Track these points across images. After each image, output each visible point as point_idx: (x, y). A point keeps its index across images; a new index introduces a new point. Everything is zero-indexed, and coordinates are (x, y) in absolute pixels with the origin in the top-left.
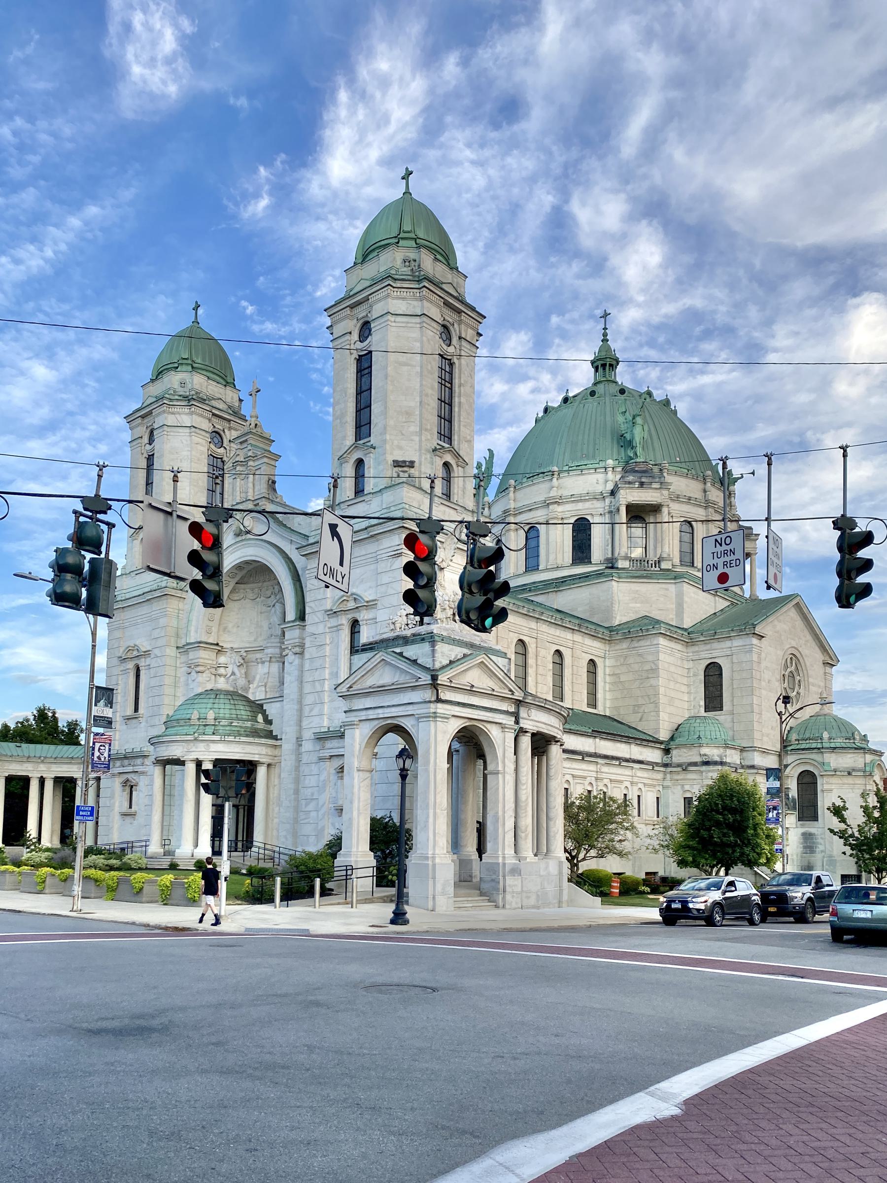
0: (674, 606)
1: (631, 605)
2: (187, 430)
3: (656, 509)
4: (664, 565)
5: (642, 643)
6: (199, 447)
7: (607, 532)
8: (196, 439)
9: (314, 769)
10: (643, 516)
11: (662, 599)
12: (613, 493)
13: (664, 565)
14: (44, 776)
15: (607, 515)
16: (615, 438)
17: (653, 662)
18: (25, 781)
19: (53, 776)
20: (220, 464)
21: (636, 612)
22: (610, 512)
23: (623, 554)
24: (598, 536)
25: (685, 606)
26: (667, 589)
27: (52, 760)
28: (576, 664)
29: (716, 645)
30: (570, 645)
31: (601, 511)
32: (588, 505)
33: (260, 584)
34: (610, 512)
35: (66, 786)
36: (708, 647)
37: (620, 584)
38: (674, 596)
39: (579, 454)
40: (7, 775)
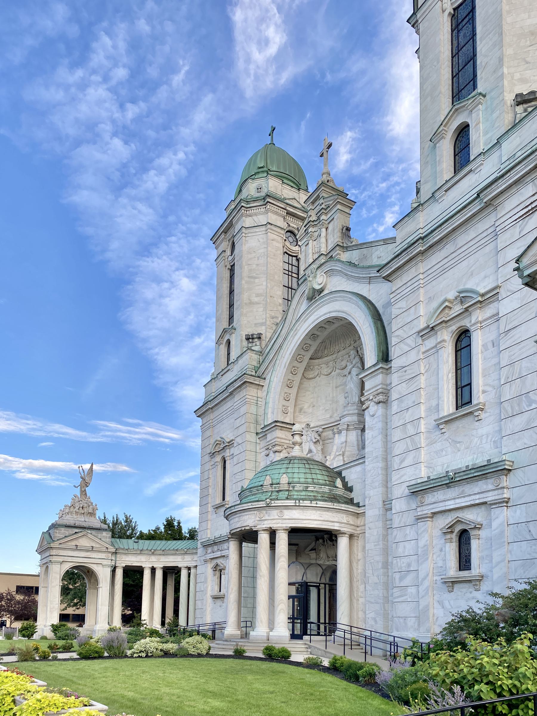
2: (264, 228)
6: (275, 243)
8: (271, 236)
9: (410, 532)
14: (155, 566)
18: (139, 571)
19: (162, 566)
20: (295, 262)
27: (161, 552)
33: (334, 356)
35: (171, 573)
40: (124, 565)
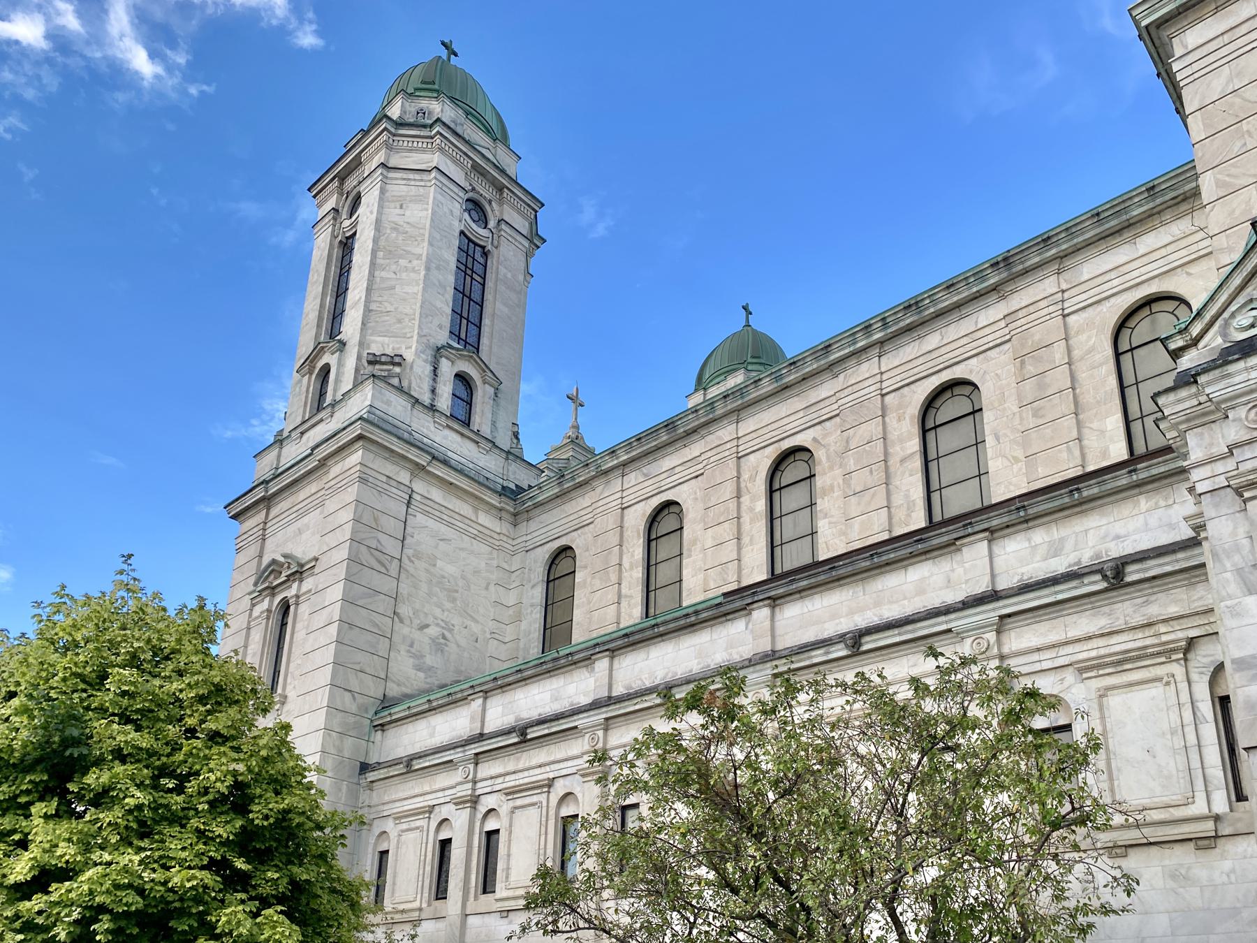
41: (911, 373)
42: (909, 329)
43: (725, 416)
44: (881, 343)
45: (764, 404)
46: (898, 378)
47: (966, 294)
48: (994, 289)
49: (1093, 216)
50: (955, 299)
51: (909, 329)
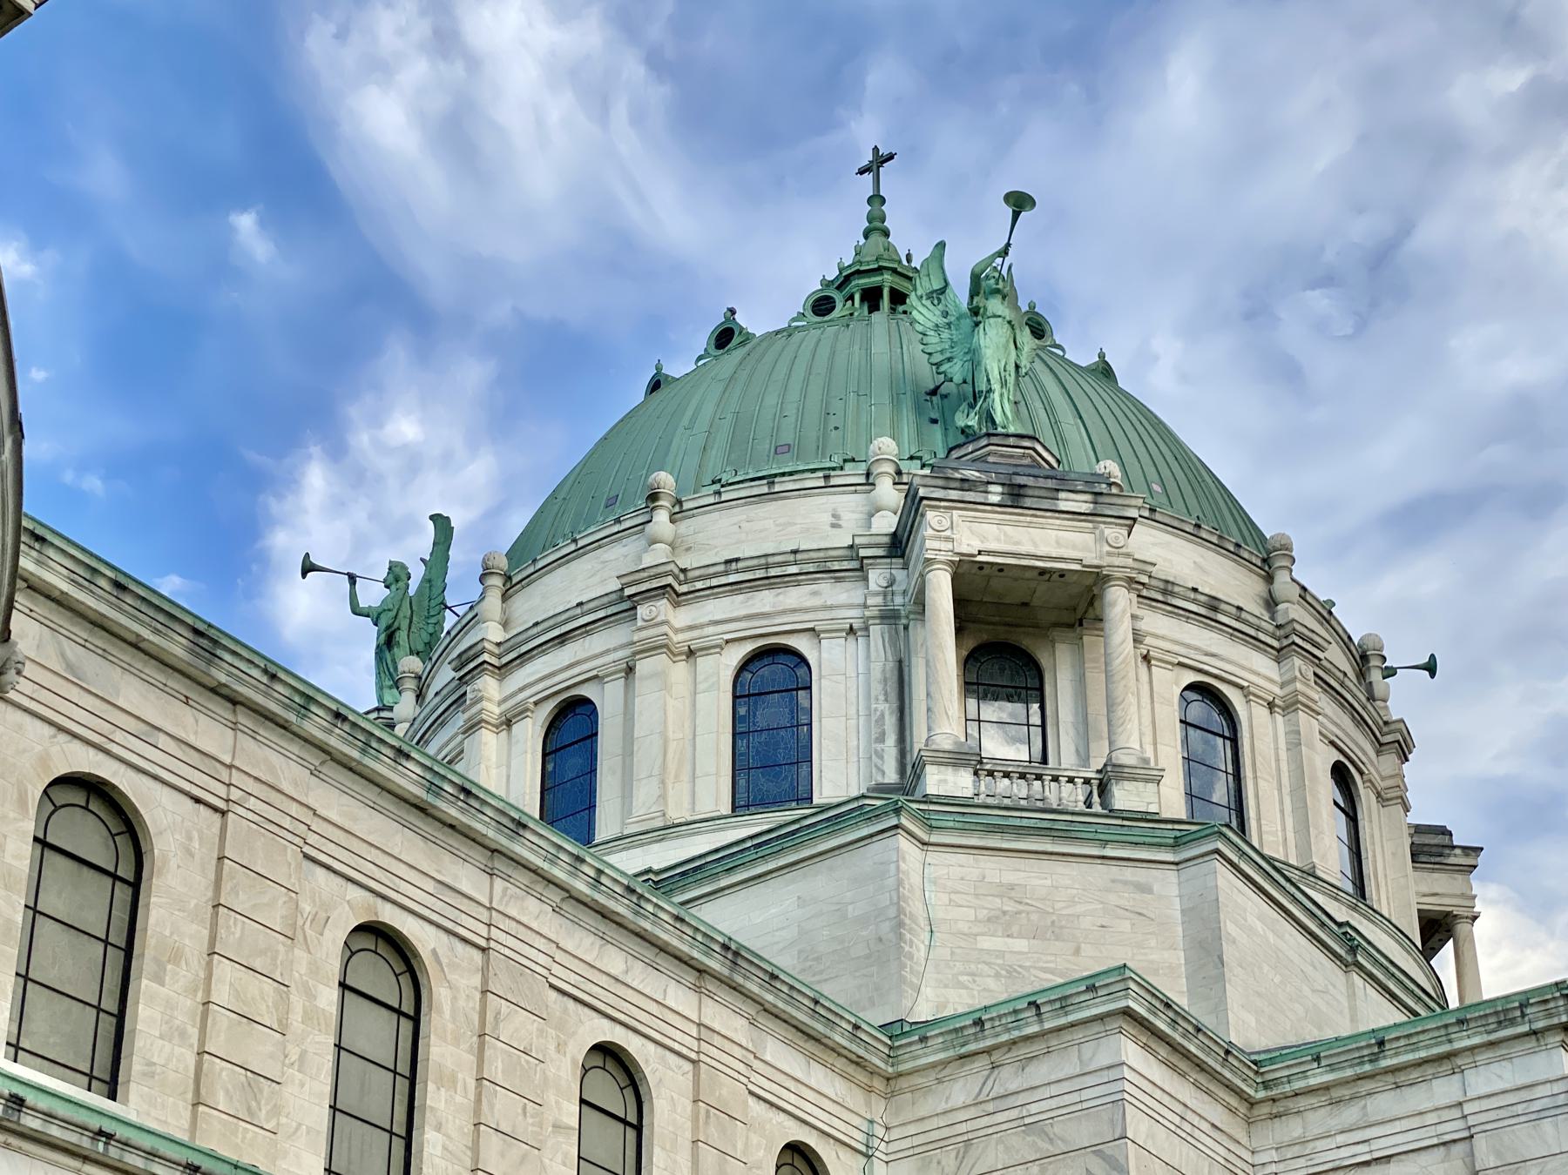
0: (1179, 957)
1: (986, 943)
3: (1073, 603)
4: (1125, 797)
5: (1040, 1072)
7: (877, 688)
10: (1027, 643)
11: (1125, 926)
12: (898, 546)
13: (1125, 797)
15: (876, 630)
16: (907, 402)
17: (1096, 1149)
21: (1011, 973)
22: (889, 617)
23: (947, 745)
24: (842, 689)
25: (1229, 953)
26: (1145, 889)
28: (713, 1134)
29: (1385, 1103)
30: (687, 1043)
31: (853, 615)
32: (794, 597)
34: (889, 617)
36: (1350, 1114)
37: (934, 857)
38: (1178, 914)
39: (765, 446)
41: (774, 1088)
42: (604, 914)
43: (308, 741)
44: (571, 896)
45: (371, 793)
46: (573, 978)
47: (685, 948)
48: (701, 971)
49: (302, 694)
50: (695, 954)
51: (604, 914)
